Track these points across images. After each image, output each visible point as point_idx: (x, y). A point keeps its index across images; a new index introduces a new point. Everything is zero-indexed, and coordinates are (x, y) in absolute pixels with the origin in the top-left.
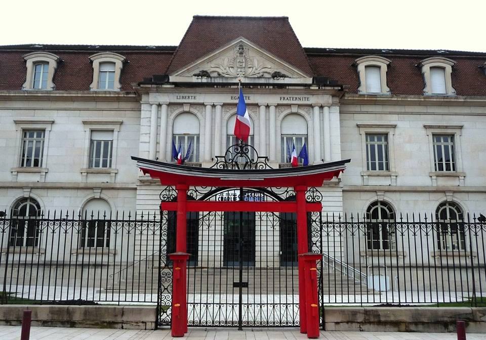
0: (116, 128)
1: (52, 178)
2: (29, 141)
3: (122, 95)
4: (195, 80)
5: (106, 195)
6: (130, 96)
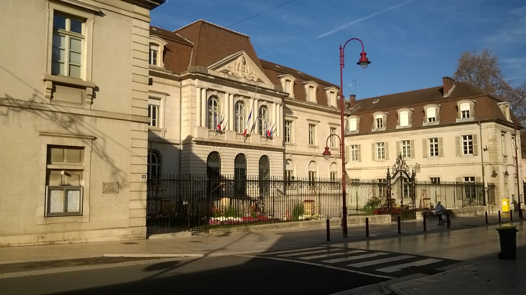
0: (163, 97)
4: (222, 75)
6: (175, 75)
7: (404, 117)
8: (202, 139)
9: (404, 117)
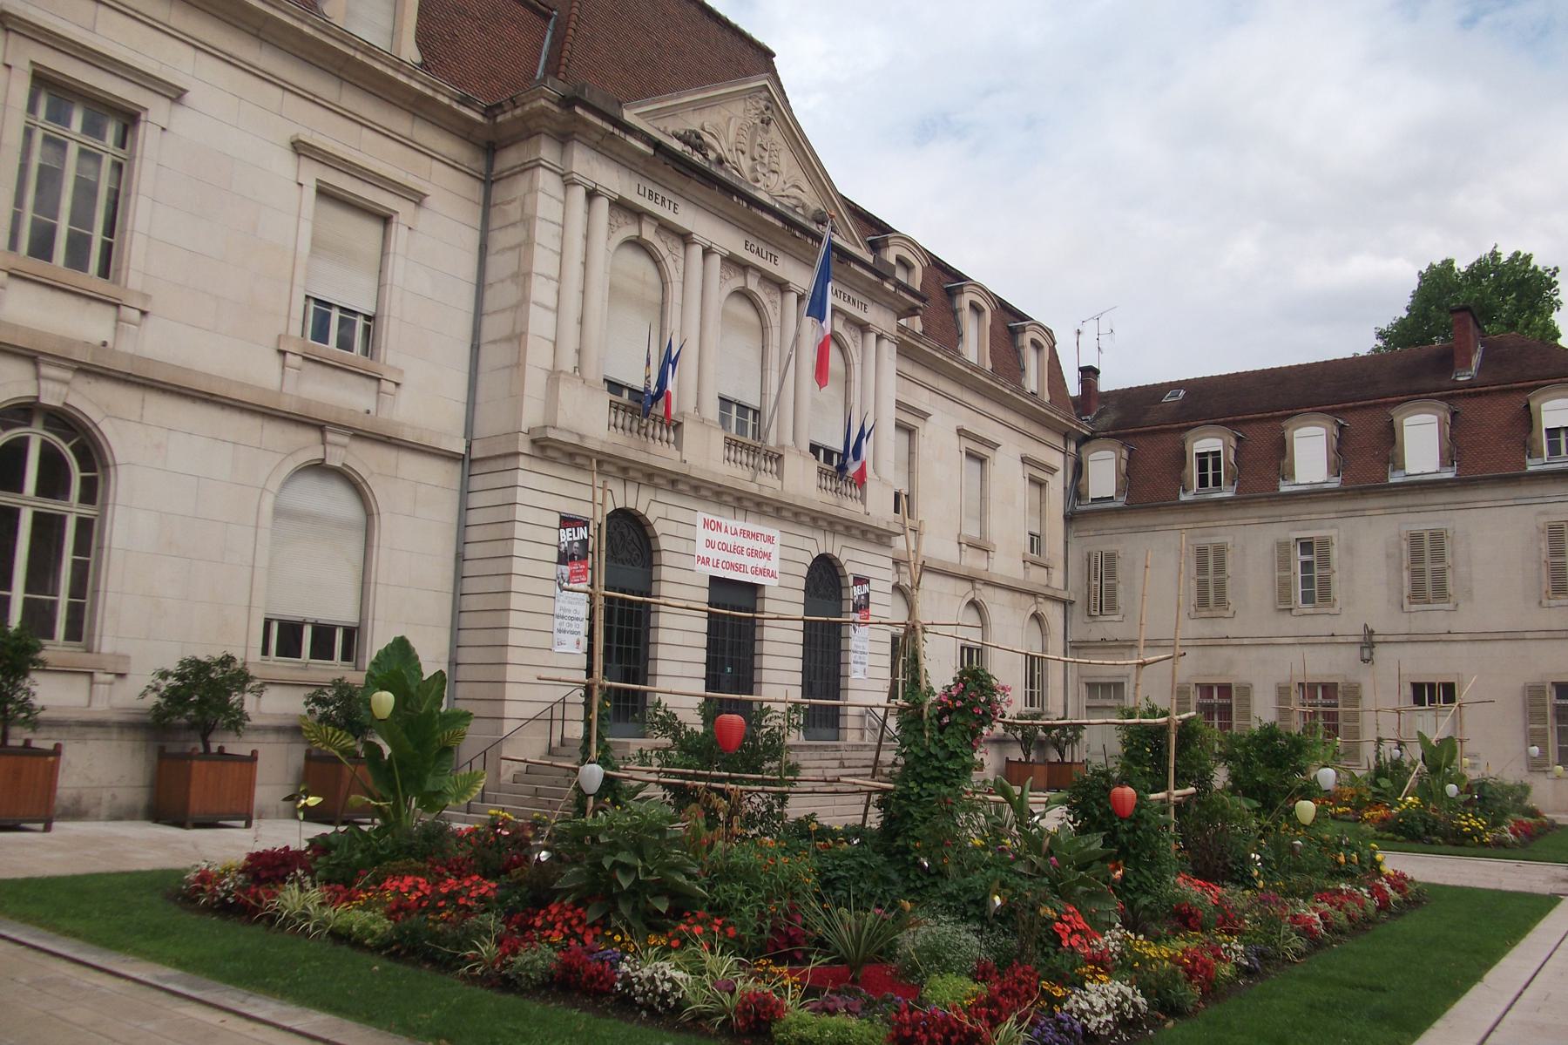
1: (157, 343)
2: (47, 139)
3: (446, 101)
5: (364, 459)
7: (1310, 452)
8: (581, 437)
9: (1310, 452)
